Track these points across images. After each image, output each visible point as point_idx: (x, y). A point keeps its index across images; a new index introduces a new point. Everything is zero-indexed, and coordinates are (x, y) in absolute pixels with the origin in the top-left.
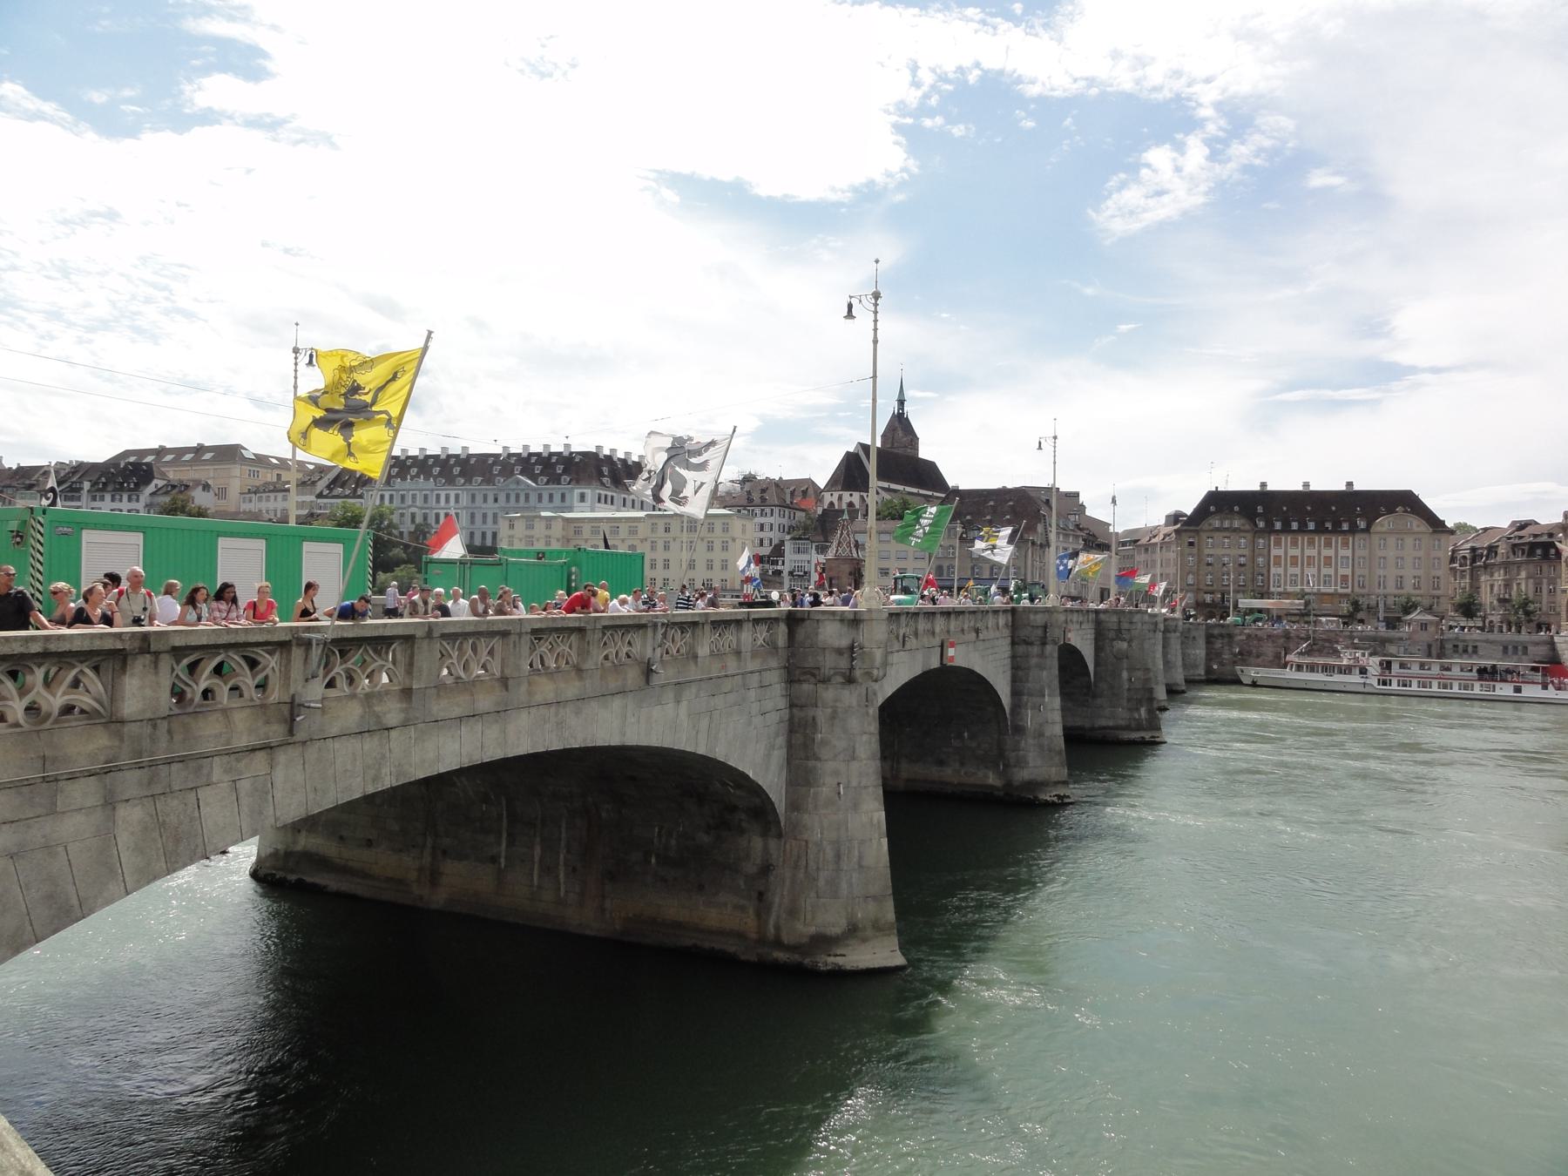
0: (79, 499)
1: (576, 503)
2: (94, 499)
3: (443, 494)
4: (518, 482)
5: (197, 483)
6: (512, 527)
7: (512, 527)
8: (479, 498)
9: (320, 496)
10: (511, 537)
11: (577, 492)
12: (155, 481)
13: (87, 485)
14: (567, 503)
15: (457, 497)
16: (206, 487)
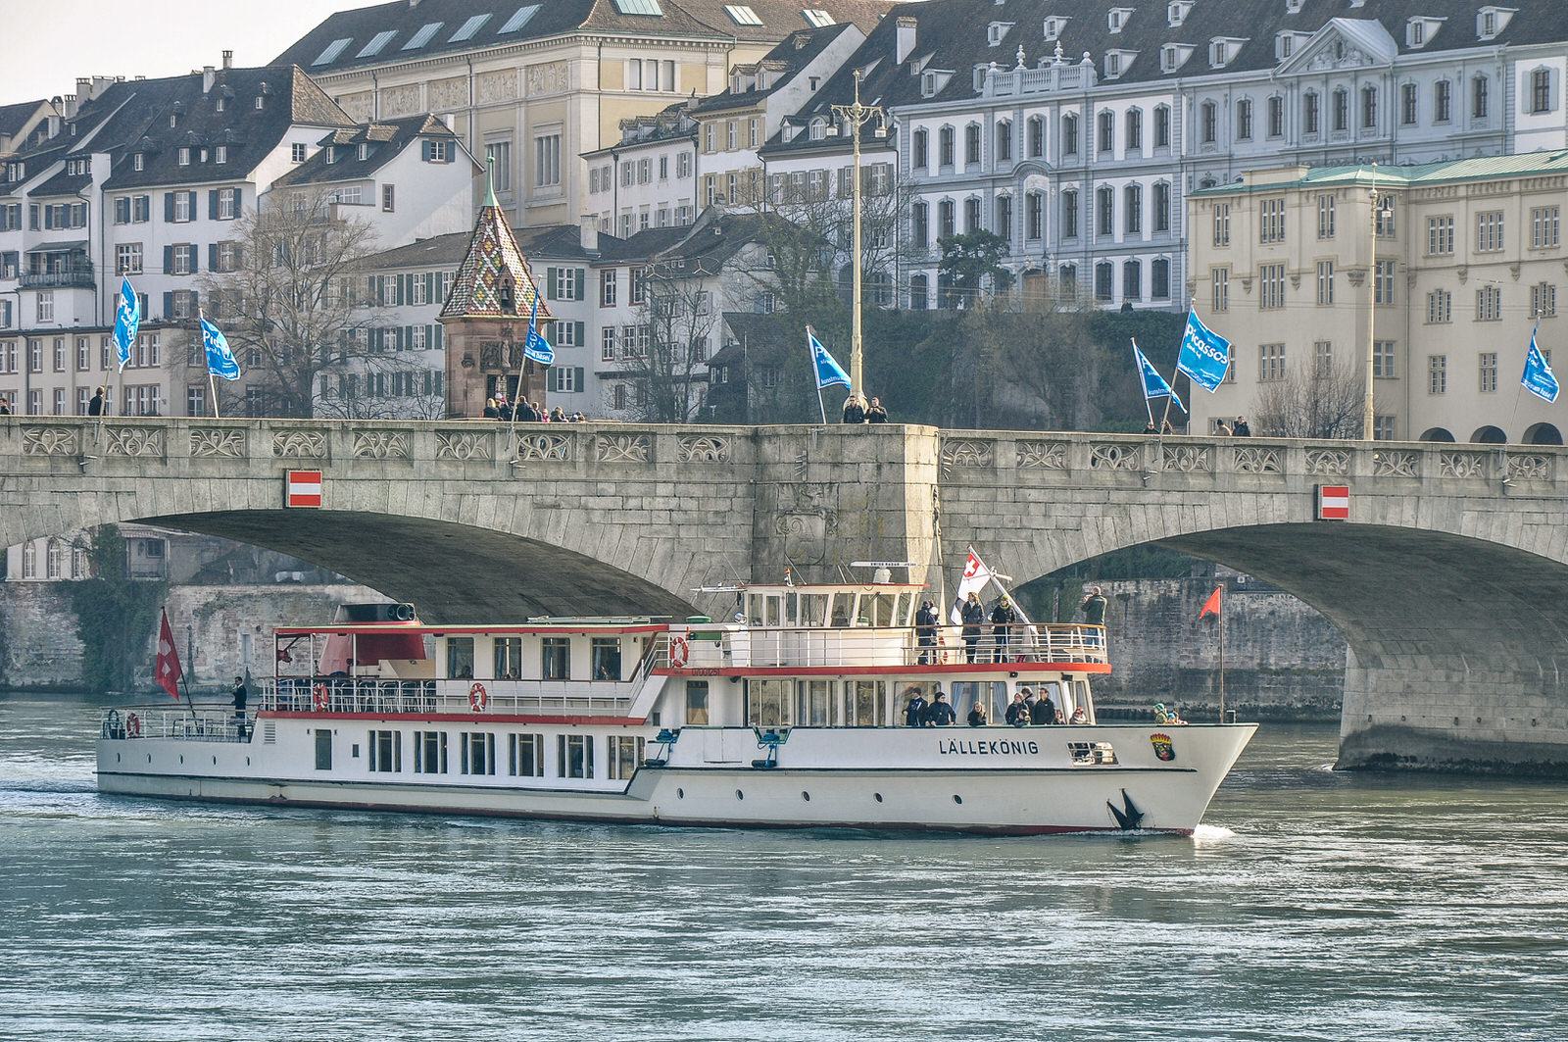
0: (81, 219)
1: (1523, 120)
2: (123, 217)
3: (1120, 109)
4: (1340, 47)
5: (408, 129)
6: (1272, 232)
7: (1272, 232)
8: (1226, 121)
9: (774, 148)
10: (1220, 273)
11: (1524, 67)
12: (294, 135)
13: (101, 166)
14: (1494, 121)
15: (1161, 114)
16: (441, 147)
